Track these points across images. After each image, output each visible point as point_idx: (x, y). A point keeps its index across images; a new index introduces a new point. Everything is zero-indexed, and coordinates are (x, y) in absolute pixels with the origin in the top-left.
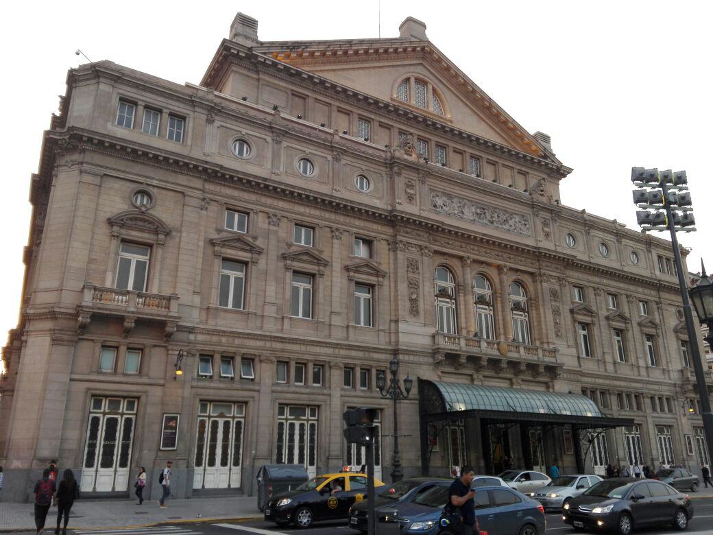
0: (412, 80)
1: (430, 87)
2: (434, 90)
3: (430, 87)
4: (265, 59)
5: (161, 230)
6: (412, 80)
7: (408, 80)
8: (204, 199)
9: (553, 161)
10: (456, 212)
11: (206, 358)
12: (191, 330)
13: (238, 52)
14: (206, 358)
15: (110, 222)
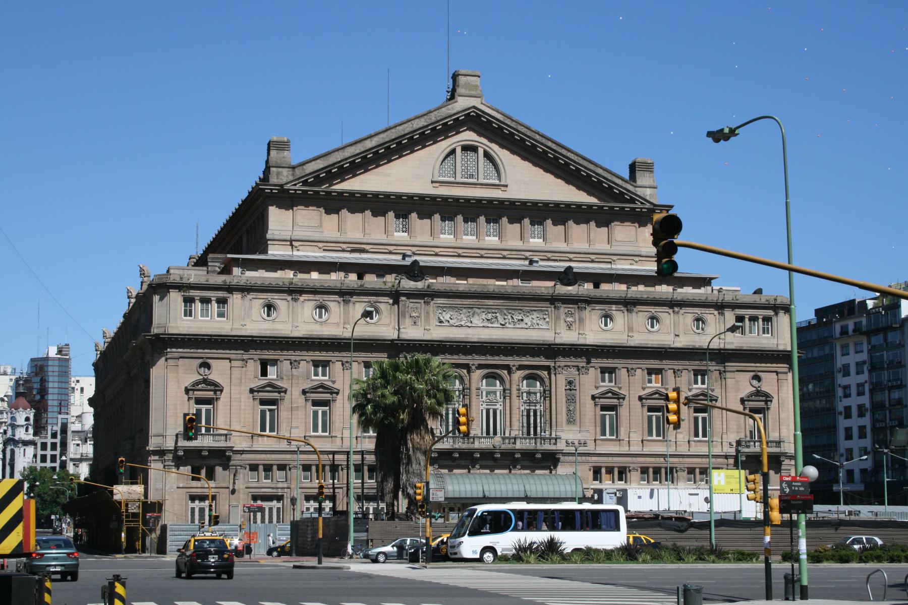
0: (459, 150)
1: (481, 151)
2: (487, 155)
3: (481, 151)
4: (296, 190)
5: (217, 388)
6: (459, 150)
7: (453, 152)
8: (243, 360)
9: (642, 203)
10: (463, 323)
11: (254, 468)
12: (242, 452)
13: (272, 190)
14: (254, 468)
15: (187, 391)
